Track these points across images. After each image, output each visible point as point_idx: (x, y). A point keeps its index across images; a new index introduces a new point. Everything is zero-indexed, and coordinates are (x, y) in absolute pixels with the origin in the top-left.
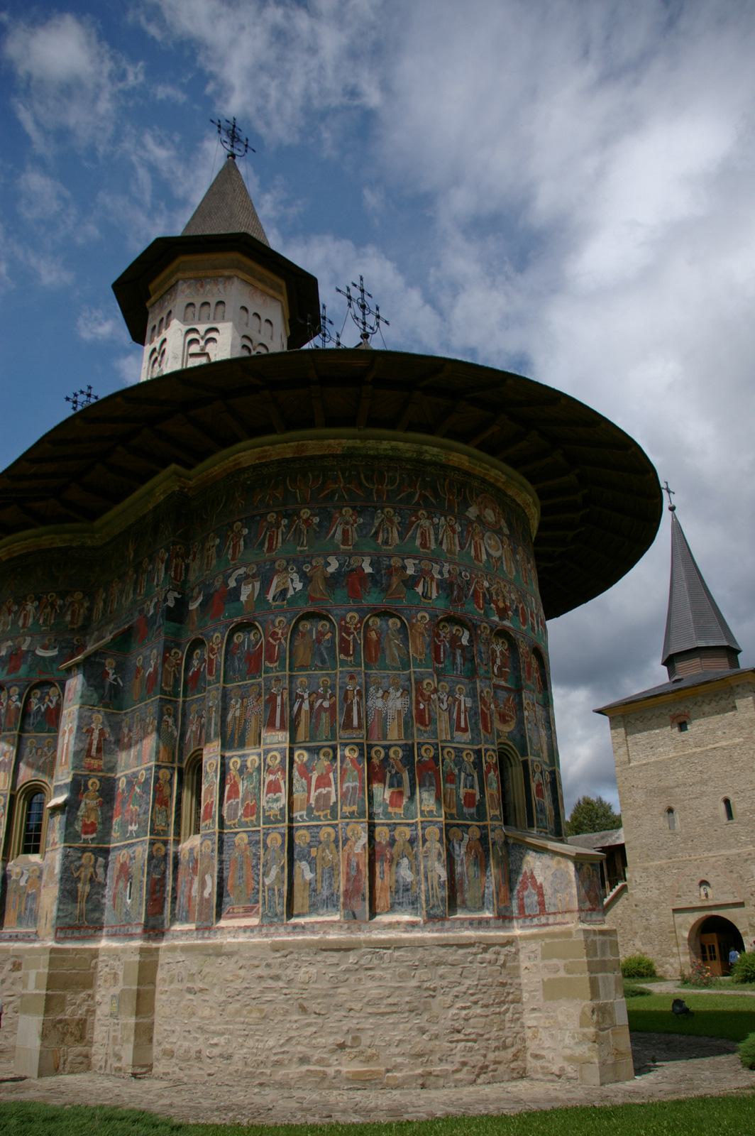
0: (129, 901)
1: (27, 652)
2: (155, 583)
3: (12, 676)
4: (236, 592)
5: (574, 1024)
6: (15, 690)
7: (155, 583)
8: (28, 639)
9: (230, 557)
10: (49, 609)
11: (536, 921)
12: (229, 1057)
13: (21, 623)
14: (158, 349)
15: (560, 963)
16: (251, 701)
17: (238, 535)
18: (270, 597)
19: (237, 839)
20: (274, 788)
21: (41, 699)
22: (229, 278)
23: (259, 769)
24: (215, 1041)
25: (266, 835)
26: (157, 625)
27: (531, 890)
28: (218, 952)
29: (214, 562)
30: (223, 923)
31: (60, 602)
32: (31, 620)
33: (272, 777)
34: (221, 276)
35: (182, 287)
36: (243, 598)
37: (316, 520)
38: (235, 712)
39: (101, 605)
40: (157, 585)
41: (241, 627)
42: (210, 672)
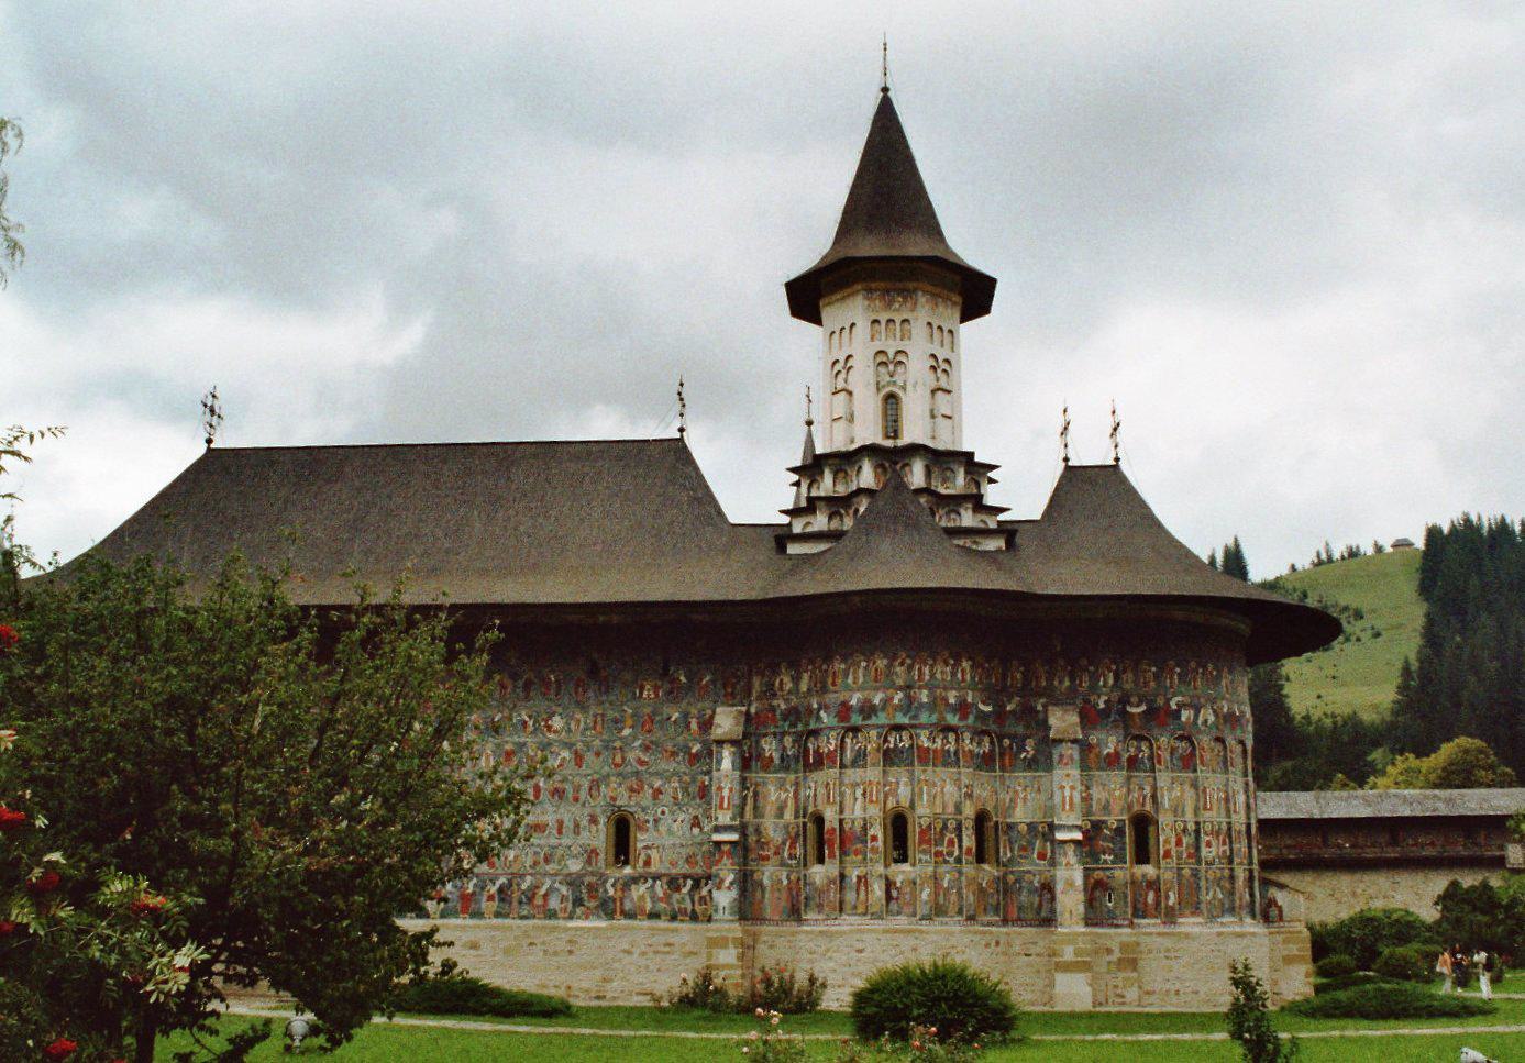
0: (1110, 904)
1: (973, 704)
2: (1101, 683)
3: (961, 724)
4: (1177, 714)
5: (1301, 977)
6: (967, 736)
7: (1101, 683)
8: (970, 693)
9: (1168, 684)
10: (980, 670)
11: (1276, 925)
12: (1197, 992)
13: (959, 675)
14: (891, 357)
15: (1295, 947)
16: (1187, 787)
17: (1172, 671)
18: (1200, 722)
19: (1184, 871)
20: (1209, 844)
21: (979, 744)
22: (954, 304)
23: (1197, 832)
24: (1188, 984)
25: (1206, 871)
26: (1112, 719)
27: (1274, 908)
28: (1187, 936)
29: (1152, 684)
30: (1180, 920)
31: (987, 665)
32: (968, 677)
33: (1208, 838)
34: (951, 300)
35: (922, 299)
36: (1183, 719)
37: (1215, 673)
38: (1177, 792)
39: (1019, 676)
40: (1104, 686)
41: (1181, 738)
42: (1159, 762)
